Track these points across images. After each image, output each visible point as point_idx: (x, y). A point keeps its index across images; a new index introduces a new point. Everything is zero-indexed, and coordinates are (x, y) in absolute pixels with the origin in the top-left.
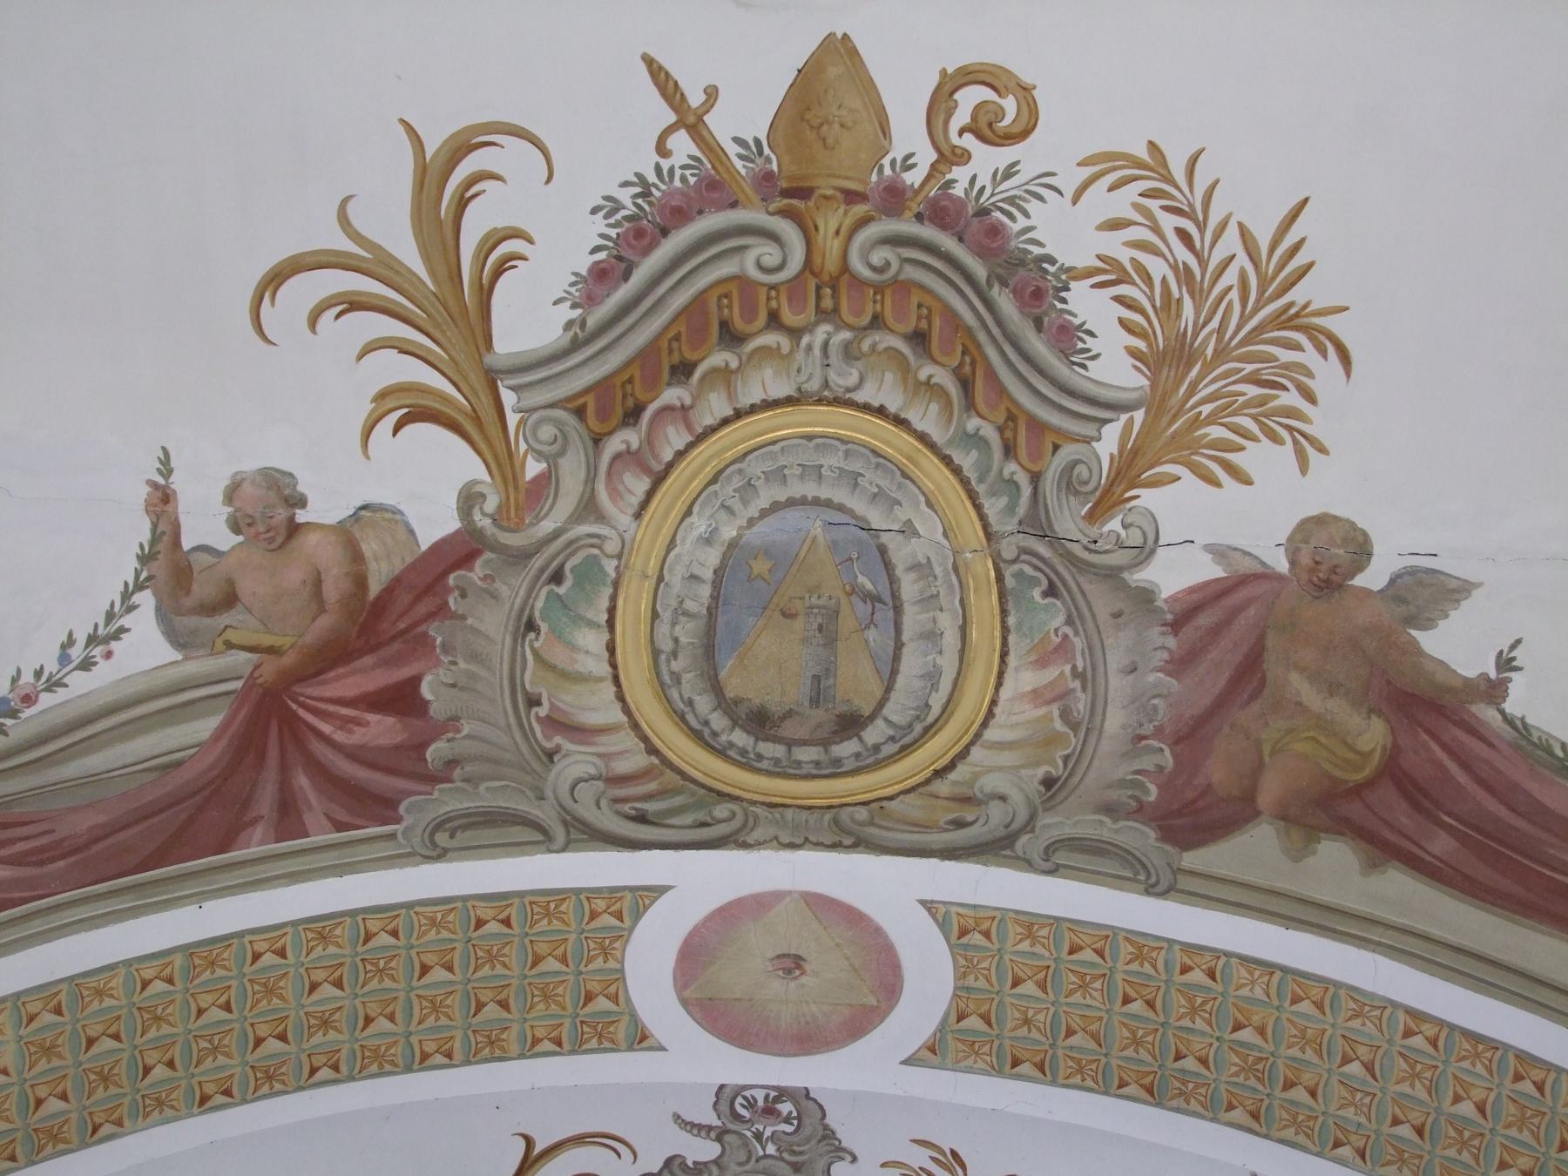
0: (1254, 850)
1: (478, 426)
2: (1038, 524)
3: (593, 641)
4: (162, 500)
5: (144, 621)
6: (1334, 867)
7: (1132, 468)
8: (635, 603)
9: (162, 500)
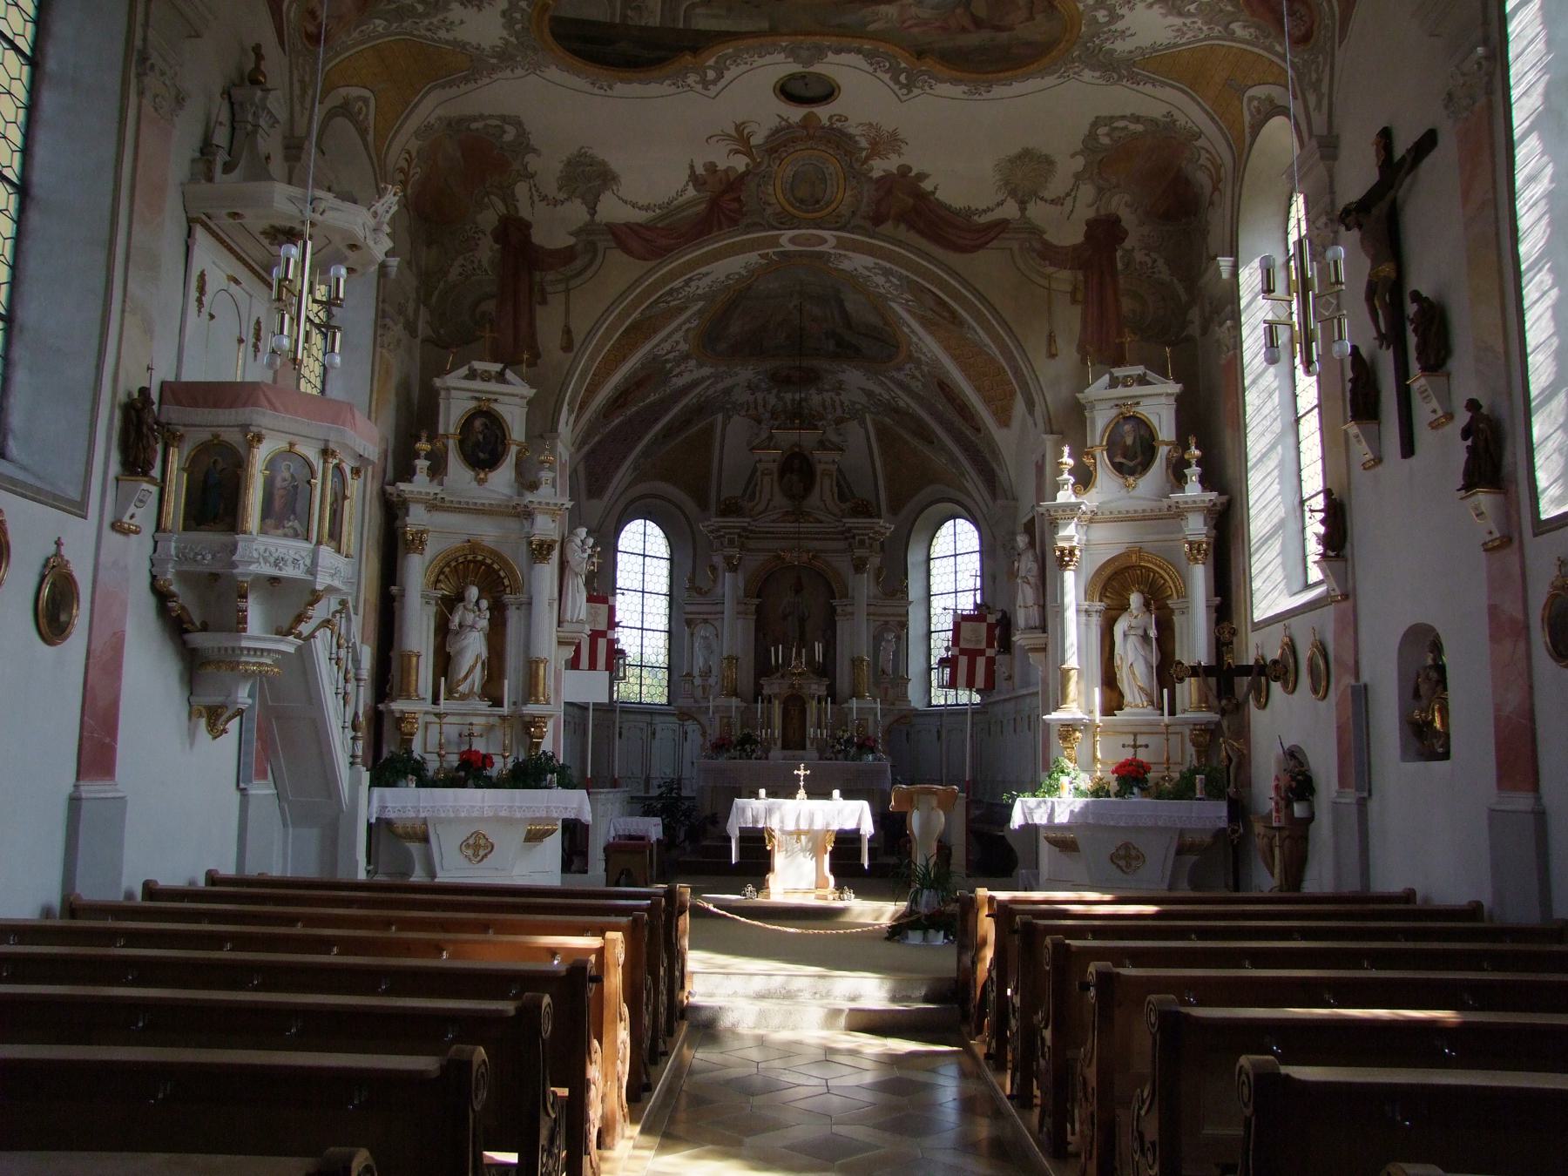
0: (887, 228)
1: (748, 154)
2: (851, 166)
3: (771, 189)
4: (692, 167)
5: (691, 187)
6: (902, 232)
7: (868, 158)
8: (778, 183)
9: (692, 167)
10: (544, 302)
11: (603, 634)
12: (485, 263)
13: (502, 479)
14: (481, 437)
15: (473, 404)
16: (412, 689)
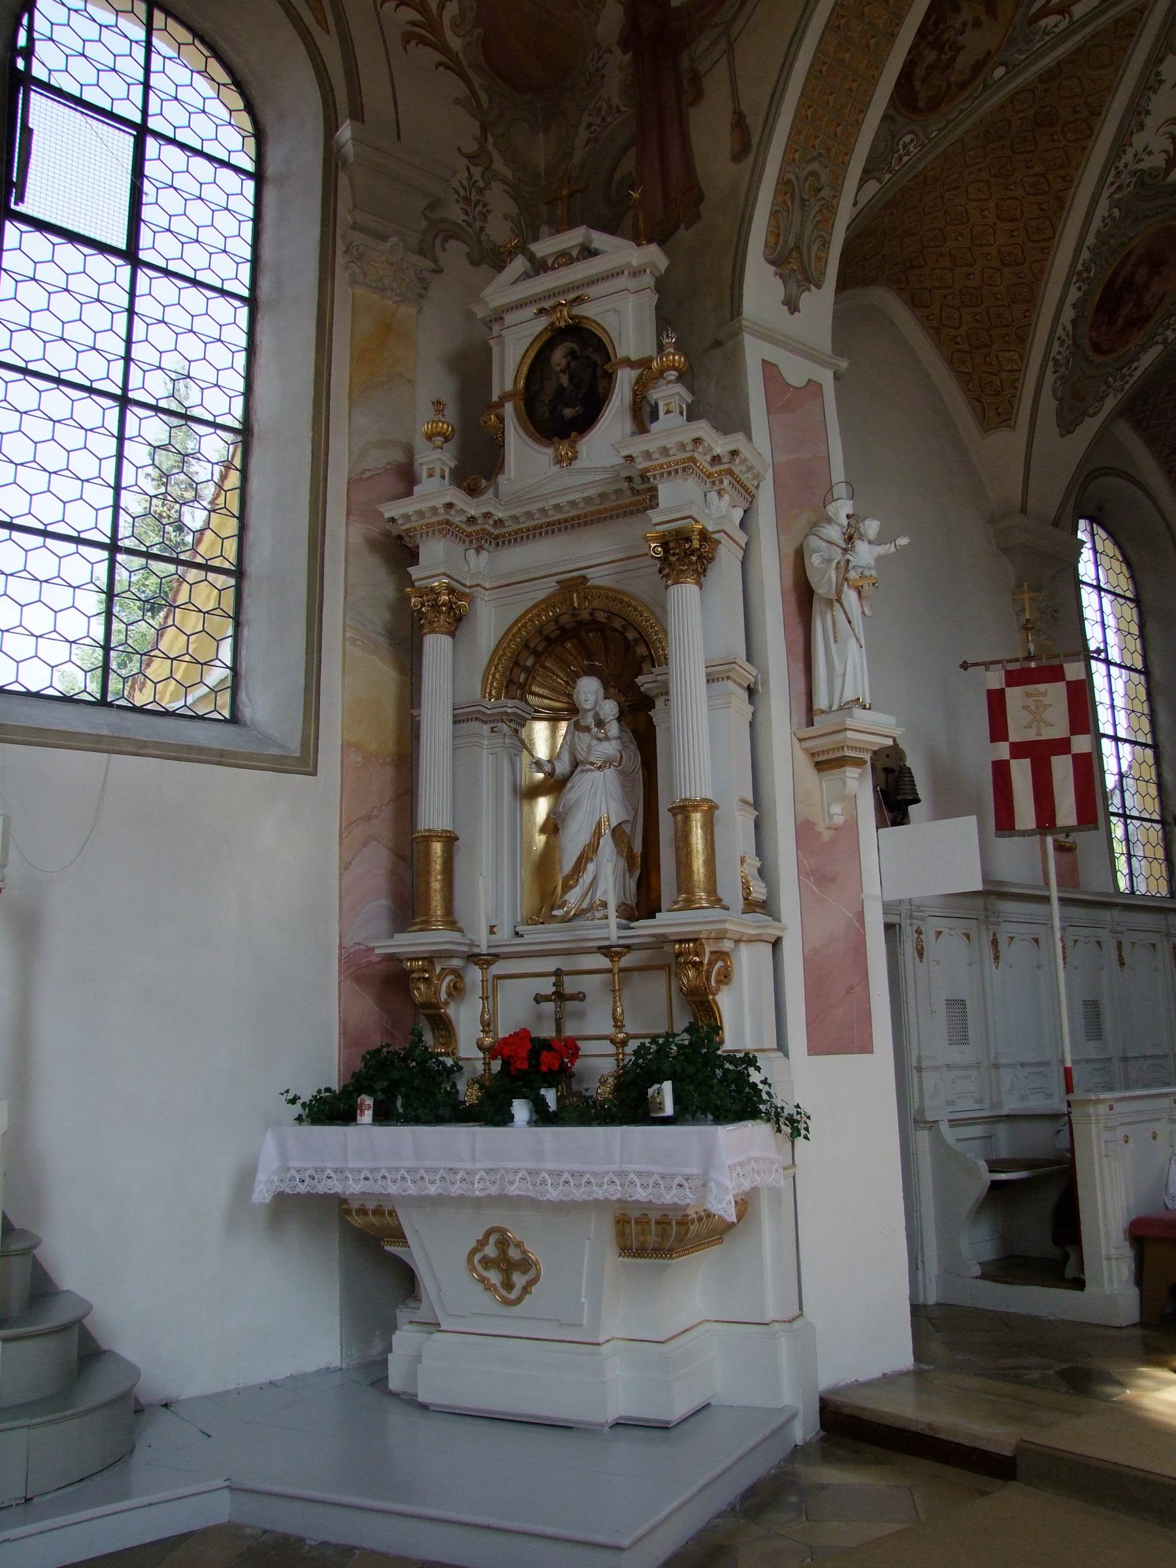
10: (699, 95)
11: (1062, 746)
12: (616, 101)
13: (607, 442)
14: (564, 380)
15: (543, 322)
16: (437, 902)
